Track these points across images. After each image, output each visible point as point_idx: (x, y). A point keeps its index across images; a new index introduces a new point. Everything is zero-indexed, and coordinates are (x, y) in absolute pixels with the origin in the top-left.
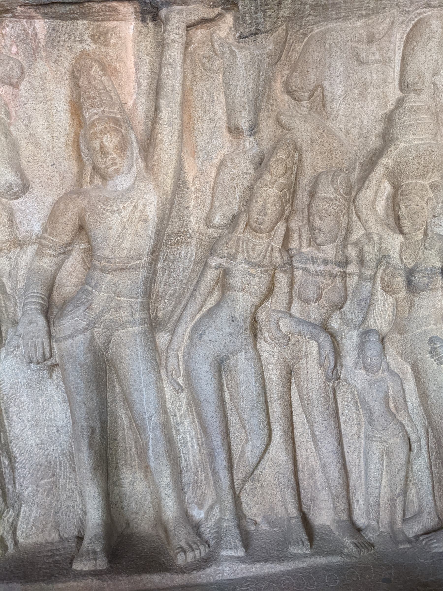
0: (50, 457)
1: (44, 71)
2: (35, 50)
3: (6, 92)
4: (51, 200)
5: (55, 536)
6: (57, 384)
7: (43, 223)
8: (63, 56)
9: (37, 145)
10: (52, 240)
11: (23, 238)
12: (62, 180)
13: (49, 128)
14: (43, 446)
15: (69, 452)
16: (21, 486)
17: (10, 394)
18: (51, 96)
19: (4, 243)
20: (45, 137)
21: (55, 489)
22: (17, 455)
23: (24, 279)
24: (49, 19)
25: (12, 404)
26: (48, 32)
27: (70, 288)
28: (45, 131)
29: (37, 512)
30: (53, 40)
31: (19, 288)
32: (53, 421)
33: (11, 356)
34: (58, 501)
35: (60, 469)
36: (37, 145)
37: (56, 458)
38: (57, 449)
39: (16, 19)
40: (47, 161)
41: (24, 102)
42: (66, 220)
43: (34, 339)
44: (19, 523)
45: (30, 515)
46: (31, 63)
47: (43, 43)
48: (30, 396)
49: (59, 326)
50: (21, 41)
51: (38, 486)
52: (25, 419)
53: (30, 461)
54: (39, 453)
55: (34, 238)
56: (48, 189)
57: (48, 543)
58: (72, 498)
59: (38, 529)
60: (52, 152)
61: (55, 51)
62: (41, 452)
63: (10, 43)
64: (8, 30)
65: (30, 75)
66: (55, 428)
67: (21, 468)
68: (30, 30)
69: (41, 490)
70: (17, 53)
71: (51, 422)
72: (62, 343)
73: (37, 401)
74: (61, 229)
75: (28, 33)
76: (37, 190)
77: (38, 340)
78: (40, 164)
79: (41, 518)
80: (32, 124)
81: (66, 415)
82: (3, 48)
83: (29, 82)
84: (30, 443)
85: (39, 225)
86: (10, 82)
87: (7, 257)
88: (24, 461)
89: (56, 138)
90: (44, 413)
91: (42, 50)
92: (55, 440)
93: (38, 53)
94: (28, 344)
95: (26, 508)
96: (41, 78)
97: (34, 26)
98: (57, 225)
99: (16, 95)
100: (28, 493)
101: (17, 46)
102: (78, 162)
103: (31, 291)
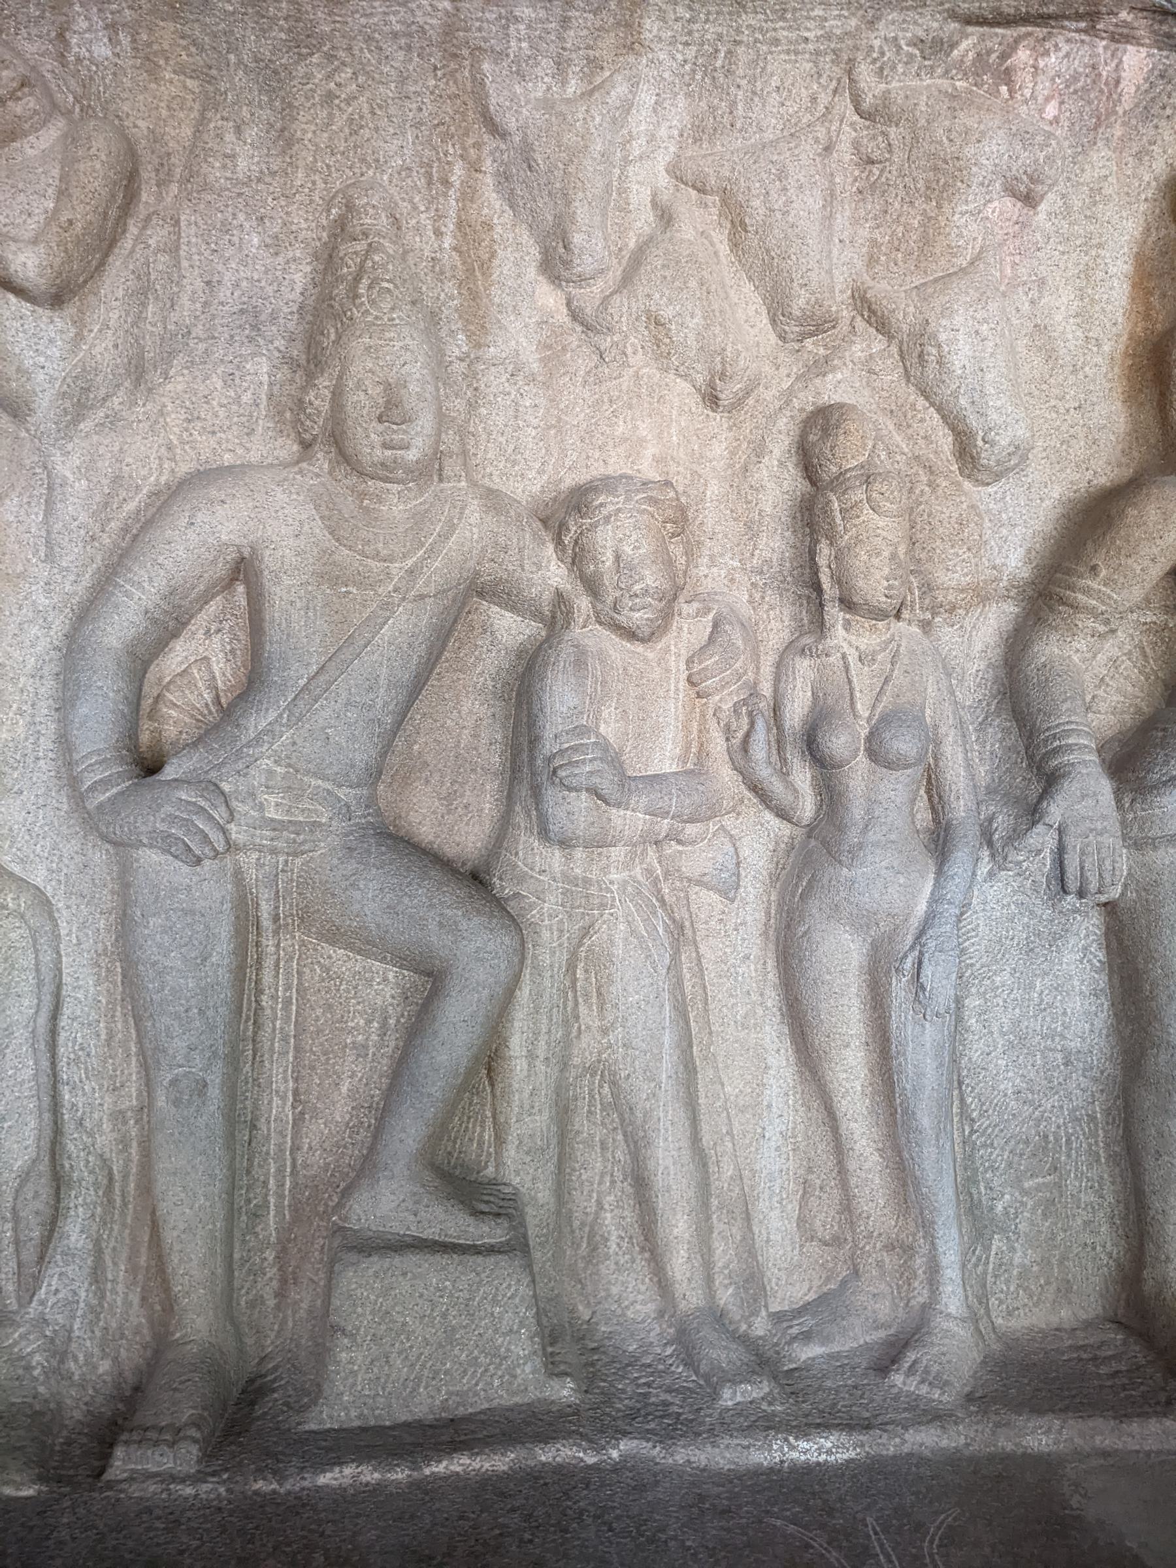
0: (1045, 1124)
1: (1104, 172)
2: (1100, 121)
3: (1001, 213)
4: (1056, 495)
5: (1065, 1315)
6: (1085, 948)
7: (1029, 551)
8: (1159, 142)
9: (1050, 355)
10: (1110, 597)
11: (985, 581)
12: (1091, 448)
13: (1083, 316)
14: (1030, 1096)
15: (1088, 1115)
16: (991, 1189)
17: (978, 966)
18: (1101, 236)
19: (962, 591)
20: (1070, 336)
21: (1060, 1202)
22: (975, 1114)
23: (979, 686)
24: (1160, 49)
25: (973, 990)
26: (1146, 80)
27: (1103, 717)
28: (1071, 320)
29: (1026, 1255)
30: (1153, 100)
31: (970, 707)
32: (1057, 1039)
33: (1011, 873)
34: (1066, 1231)
35: (1069, 1156)
36: (1050, 355)
37: (1059, 1127)
38: (1061, 1107)
39: (1083, 37)
40: (1068, 397)
41: (1037, 242)
42: (1155, 551)
43: (1091, 838)
44: (990, 1279)
45: (1012, 1259)
46: (1080, 149)
47: (1127, 103)
48: (1017, 975)
49: (1144, 810)
50: (1075, 92)
51: (1025, 1192)
52: (995, 1029)
53: (1002, 1131)
54: (1020, 1114)
55: (1005, 583)
56: (1058, 467)
57: (1057, 1329)
58: (1092, 1225)
59: (1031, 1297)
60: (1081, 376)
61: (1148, 131)
62: (1027, 1110)
63: (1046, 92)
64: (1053, 60)
65: (1069, 179)
66: (1059, 1056)
67: (984, 1146)
68: (1108, 68)
69: (1030, 1203)
70: (1056, 120)
71: (1053, 1040)
72: (1161, 852)
73: (1032, 986)
74: (1138, 572)
75: (1100, 75)
76: (1036, 470)
77: (1099, 839)
78: (1053, 402)
79: (1035, 1268)
80: (1043, 301)
81: (1092, 1024)
82: (1026, 102)
83: (1063, 196)
84: (1002, 1087)
85: (1021, 552)
86: (1030, 191)
87: (962, 627)
88: (990, 1130)
89: (1093, 341)
90: (1039, 1018)
91: (1119, 121)
92: (1060, 1084)
93: (1107, 127)
94: (1075, 847)
95: (1001, 1244)
96: (1091, 189)
97: (1121, 61)
98: (1130, 561)
99: (1024, 225)
100: (1005, 1208)
101: (1062, 103)
102: (1130, 407)
103: (1064, 719)
